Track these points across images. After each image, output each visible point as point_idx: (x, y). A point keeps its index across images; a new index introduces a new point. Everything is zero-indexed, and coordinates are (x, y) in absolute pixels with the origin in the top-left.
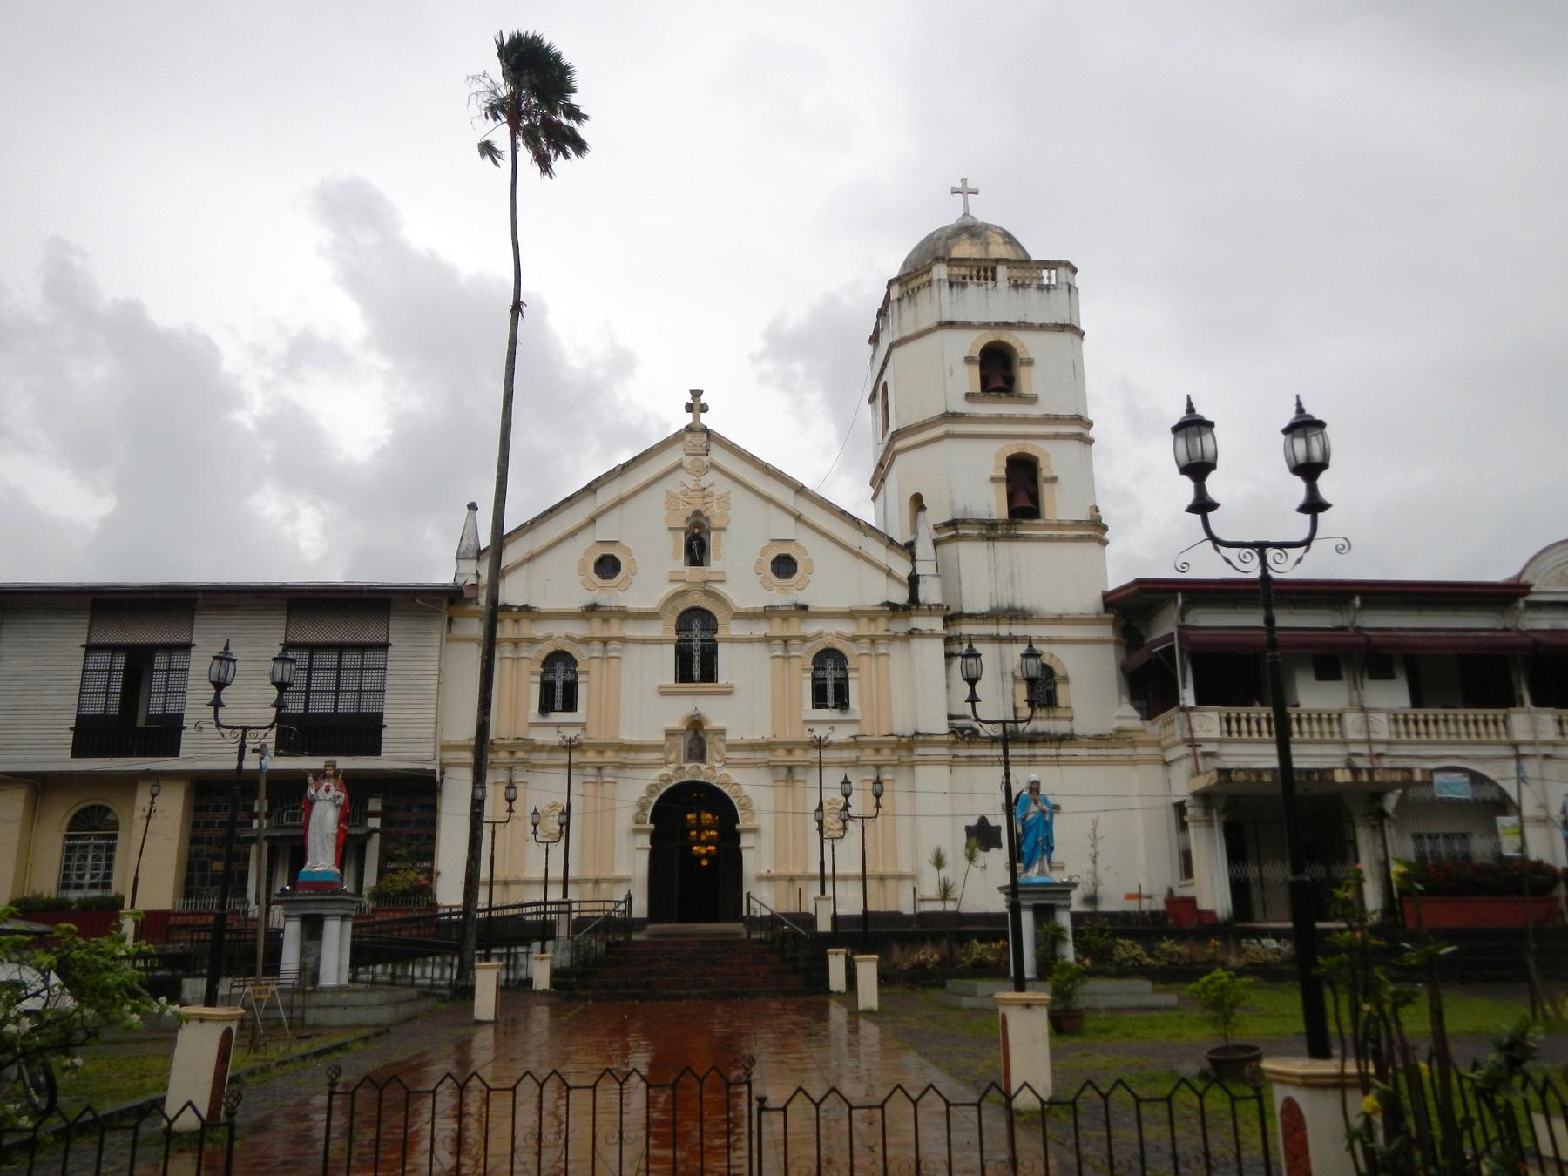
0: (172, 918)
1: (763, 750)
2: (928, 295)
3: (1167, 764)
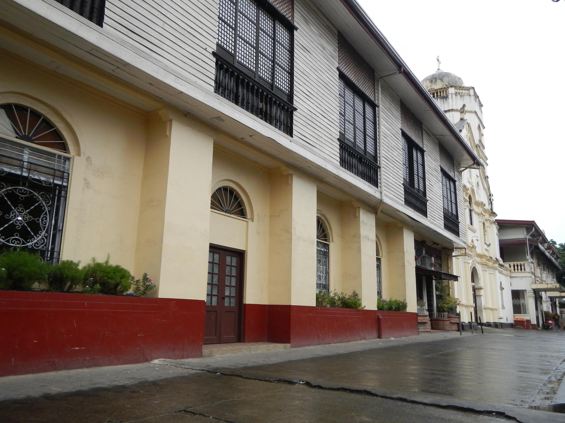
0: (419, 318)
1: (479, 257)
2: (469, 98)
3: (511, 277)
